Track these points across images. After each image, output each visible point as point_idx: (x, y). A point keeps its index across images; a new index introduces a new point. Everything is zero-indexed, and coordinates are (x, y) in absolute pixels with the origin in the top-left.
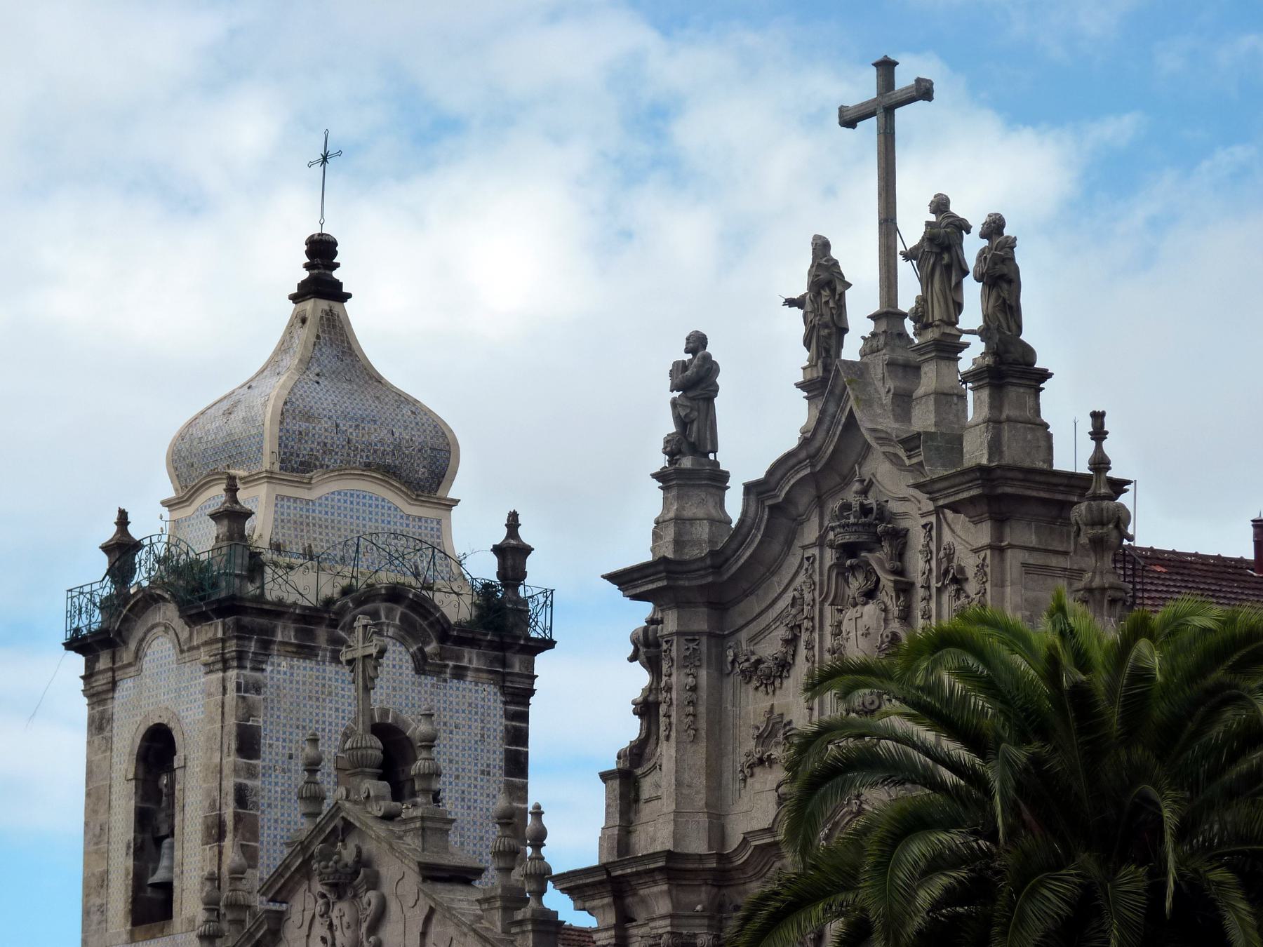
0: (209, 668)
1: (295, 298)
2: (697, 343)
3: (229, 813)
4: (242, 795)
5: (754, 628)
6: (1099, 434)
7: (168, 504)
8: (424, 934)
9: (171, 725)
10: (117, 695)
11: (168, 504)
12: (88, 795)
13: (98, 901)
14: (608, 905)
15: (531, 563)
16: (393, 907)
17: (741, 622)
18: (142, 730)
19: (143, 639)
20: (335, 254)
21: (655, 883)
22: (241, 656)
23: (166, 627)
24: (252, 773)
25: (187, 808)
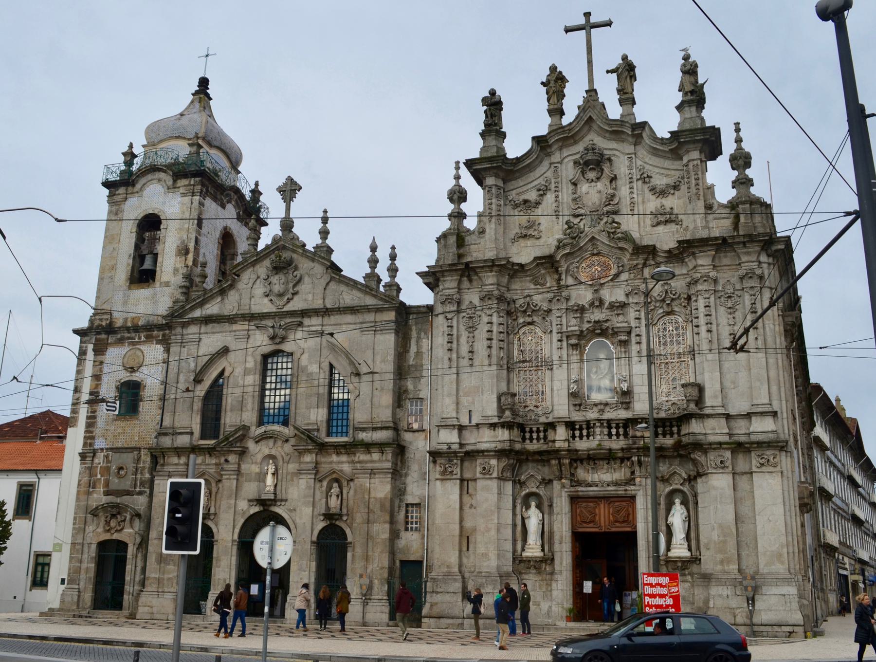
0: (184, 195)
1: (193, 95)
2: (493, 93)
3: (191, 246)
4: (197, 241)
6: (738, 130)
7: (144, 146)
8: (325, 289)
9: (159, 214)
10: (127, 203)
11: (144, 146)
12: (106, 237)
13: (110, 275)
15: (262, 198)
16: (306, 279)
17: (512, 187)
18: (145, 213)
19: (144, 184)
20: (208, 84)
21: (491, 271)
22: (201, 193)
24: (200, 235)
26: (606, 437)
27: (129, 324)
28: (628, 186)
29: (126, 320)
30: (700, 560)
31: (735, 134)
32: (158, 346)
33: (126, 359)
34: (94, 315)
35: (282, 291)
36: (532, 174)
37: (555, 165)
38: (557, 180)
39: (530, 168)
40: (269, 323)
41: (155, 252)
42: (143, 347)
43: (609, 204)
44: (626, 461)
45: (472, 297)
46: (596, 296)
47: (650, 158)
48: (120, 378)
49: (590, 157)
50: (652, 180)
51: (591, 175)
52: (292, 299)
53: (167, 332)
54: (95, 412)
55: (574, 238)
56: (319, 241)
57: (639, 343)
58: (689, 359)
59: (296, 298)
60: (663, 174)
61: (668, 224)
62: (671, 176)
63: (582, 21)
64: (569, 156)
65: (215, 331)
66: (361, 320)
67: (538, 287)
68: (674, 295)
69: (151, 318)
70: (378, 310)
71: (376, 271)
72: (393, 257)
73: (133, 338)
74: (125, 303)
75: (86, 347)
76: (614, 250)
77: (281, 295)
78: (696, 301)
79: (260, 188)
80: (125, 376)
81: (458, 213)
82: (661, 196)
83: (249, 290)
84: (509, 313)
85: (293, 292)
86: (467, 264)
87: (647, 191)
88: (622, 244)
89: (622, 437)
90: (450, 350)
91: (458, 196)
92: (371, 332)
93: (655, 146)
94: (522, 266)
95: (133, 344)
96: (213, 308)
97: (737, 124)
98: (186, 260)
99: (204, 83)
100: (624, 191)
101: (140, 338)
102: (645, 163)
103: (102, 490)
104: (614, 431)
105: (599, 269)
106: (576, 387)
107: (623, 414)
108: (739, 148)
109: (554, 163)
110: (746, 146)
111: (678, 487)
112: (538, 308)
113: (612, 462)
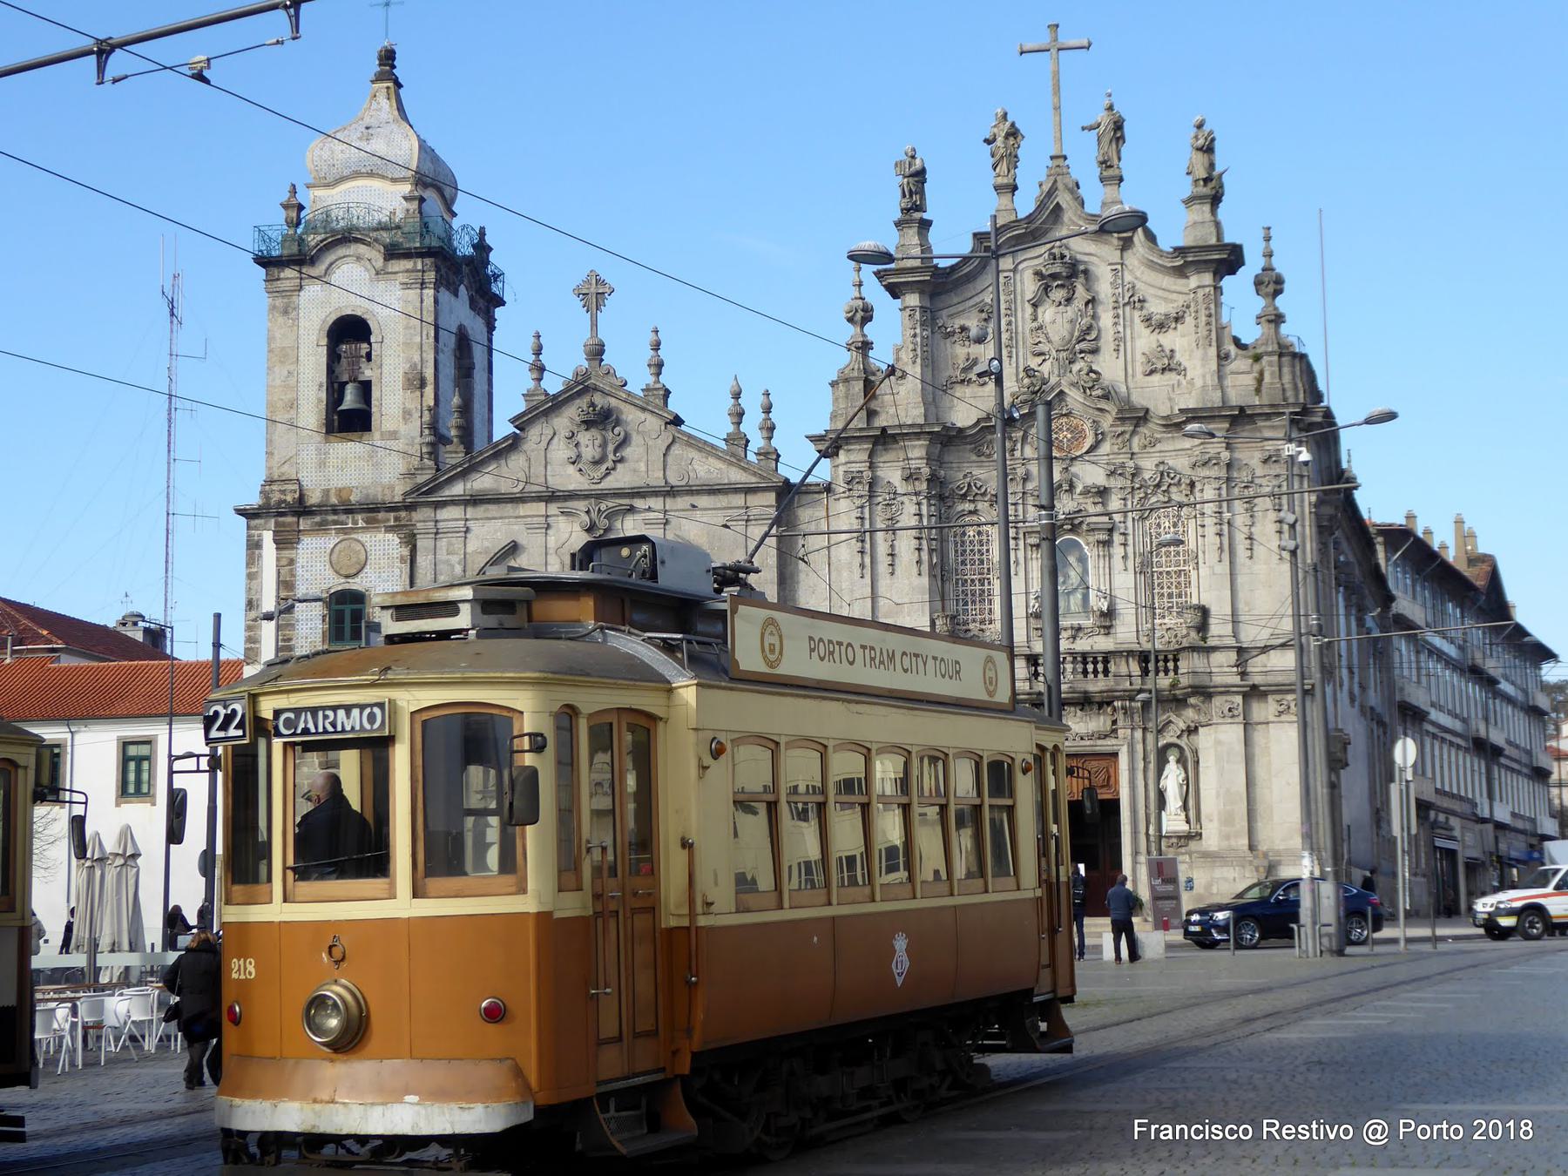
0: (406, 286)
3: (429, 373)
5: (952, 310)
6: (1268, 239)
9: (364, 316)
10: (302, 293)
13: (287, 416)
14: (867, 449)
15: (492, 257)
16: (636, 439)
18: (339, 315)
19: (331, 264)
20: (394, 59)
21: (919, 439)
23: (358, 258)
25: (384, 367)
26: (1080, 676)
27: (334, 500)
28: (1111, 313)
29: (326, 492)
30: (1201, 834)
31: (1264, 244)
32: (390, 536)
33: (335, 556)
34: (270, 482)
35: (597, 457)
36: (970, 285)
37: (1006, 274)
38: (1009, 298)
39: (971, 278)
40: (581, 505)
41: (361, 378)
42: (365, 537)
43: (1084, 340)
44: (1105, 706)
45: (891, 473)
46: (1065, 475)
47: (1143, 273)
48: (327, 586)
49: (1057, 268)
50: (1146, 305)
51: (1059, 295)
52: (614, 469)
53: (403, 514)
54: (290, 640)
55: (1036, 393)
56: (651, 380)
57: (1125, 545)
58: (1191, 568)
59: (619, 466)
60: (1161, 297)
61: (1167, 373)
62: (1172, 301)
63: (1044, 39)
64: (1025, 260)
65: (490, 516)
66: (724, 505)
67: (983, 458)
68: (1172, 479)
69: (371, 491)
70: (749, 491)
71: (743, 428)
72: (768, 409)
73: (342, 523)
74: (322, 464)
75: (260, 535)
76: (1091, 411)
77: (597, 463)
78: (1202, 491)
79: (489, 240)
80: (338, 584)
81: (863, 342)
82: (1157, 331)
83: (543, 453)
84: (941, 498)
85: (614, 458)
86: (884, 429)
87: (1137, 320)
88: (1103, 405)
89: (1101, 676)
90: (862, 552)
91: (862, 315)
92: (740, 523)
93: (1151, 258)
94: (961, 430)
95: (345, 531)
96: (482, 482)
97: (1269, 228)
98: (422, 396)
99: (388, 57)
100: (1106, 319)
101: (355, 523)
102: (1136, 278)
103: (317, 761)
104: (1090, 667)
105: (1069, 436)
106: (1037, 605)
107: (1102, 644)
108: (1268, 269)
109: (1004, 271)
110: (1276, 262)
111: (1174, 740)
112: (983, 490)
113: (1087, 707)
